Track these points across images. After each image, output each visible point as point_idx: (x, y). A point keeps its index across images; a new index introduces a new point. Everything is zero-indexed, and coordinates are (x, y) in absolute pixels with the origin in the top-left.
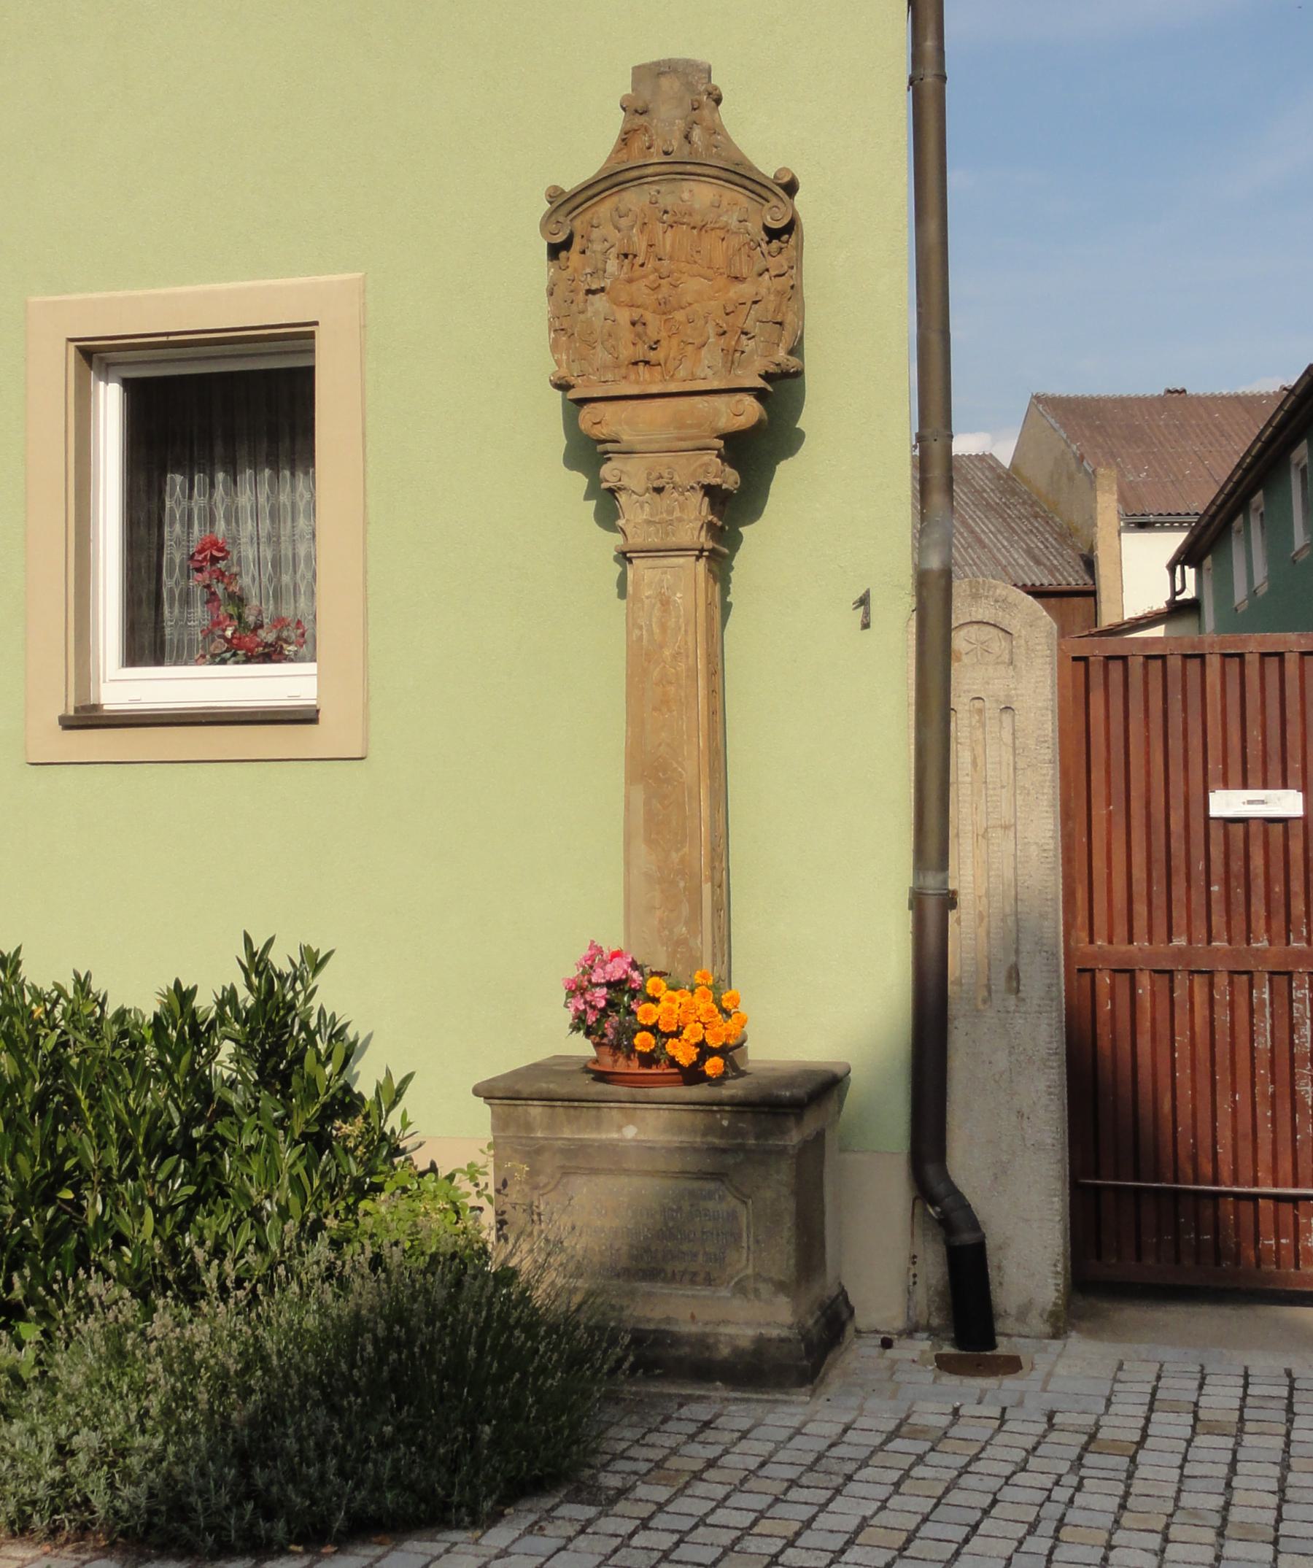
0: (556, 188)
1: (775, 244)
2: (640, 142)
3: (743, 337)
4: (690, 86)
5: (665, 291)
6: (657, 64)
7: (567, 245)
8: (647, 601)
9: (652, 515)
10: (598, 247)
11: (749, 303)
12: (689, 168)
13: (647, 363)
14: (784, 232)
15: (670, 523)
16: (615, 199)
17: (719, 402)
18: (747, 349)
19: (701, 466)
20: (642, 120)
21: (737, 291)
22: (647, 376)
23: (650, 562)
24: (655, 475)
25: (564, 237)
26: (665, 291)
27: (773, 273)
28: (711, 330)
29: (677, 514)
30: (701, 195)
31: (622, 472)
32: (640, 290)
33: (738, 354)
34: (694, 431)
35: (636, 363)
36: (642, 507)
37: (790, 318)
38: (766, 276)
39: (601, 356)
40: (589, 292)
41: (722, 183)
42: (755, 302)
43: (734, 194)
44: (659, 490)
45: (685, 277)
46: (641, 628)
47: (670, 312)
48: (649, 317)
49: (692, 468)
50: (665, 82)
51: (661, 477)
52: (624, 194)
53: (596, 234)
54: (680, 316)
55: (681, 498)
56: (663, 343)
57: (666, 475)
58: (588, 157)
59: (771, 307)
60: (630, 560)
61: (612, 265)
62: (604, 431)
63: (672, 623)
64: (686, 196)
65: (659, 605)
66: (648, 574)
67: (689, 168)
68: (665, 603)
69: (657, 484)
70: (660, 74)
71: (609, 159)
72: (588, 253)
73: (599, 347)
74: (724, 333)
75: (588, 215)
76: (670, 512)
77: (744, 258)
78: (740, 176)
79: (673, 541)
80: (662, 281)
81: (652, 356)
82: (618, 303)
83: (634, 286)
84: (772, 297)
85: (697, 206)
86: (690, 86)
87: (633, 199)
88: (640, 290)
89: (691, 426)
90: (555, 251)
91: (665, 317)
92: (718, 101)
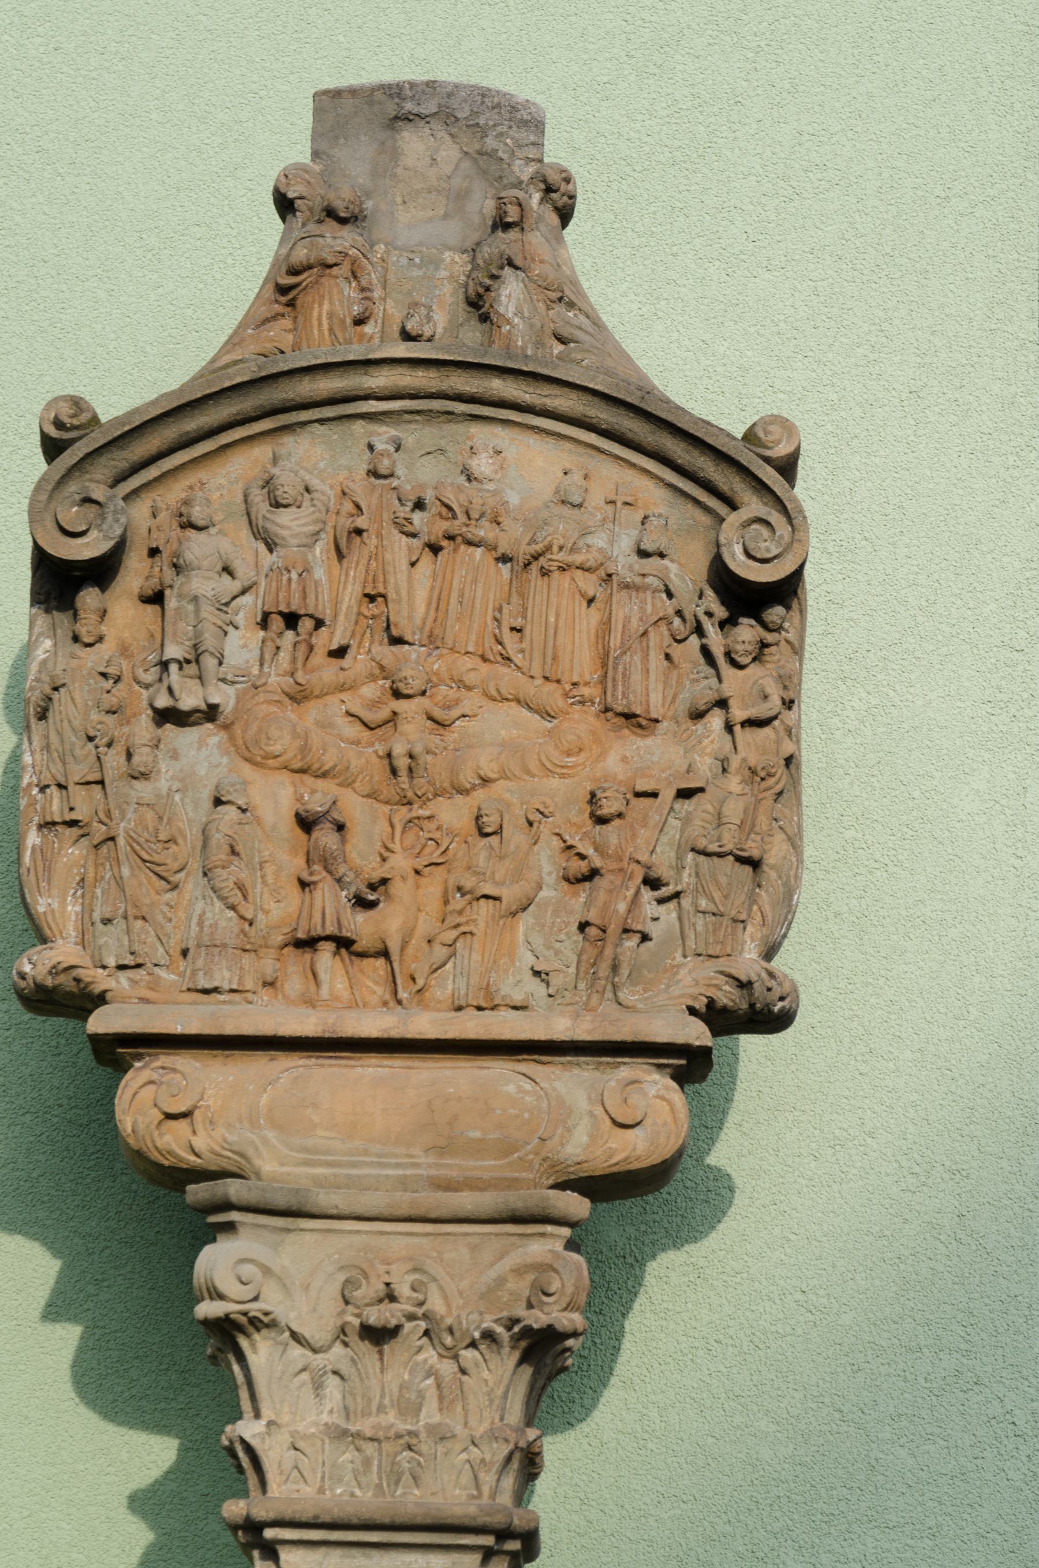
0: (77, 403)
1: (747, 632)
2: (332, 301)
3: (647, 894)
4: (486, 162)
5: (412, 733)
6: (394, 91)
7: (102, 571)
10: (206, 585)
11: (668, 794)
12: (499, 386)
13: (343, 943)
14: (757, 600)
16: (261, 452)
17: (571, 1083)
18: (655, 930)
19: (519, 1271)
20: (338, 240)
21: (625, 758)
22: (341, 986)
24: (364, 1292)
26: (412, 733)
27: (738, 713)
28: (547, 862)
29: (430, 1414)
30: (524, 469)
31: (266, 1271)
32: (330, 727)
34: (485, 1166)
35: (308, 944)
36: (318, 1387)
37: (775, 852)
38: (716, 720)
40: (169, 716)
42: (685, 794)
43: (630, 476)
44: (378, 1335)
45: (470, 702)
47: (423, 799)
48: (354, 807)
49: (493, 1273)
50: (413, 144)
52: (288, 440)
53: (198, 548)
54: (453, 814)
55: (448, 1368)
56: (399, 889)
57: (403, 1290)
58: (167, 323)
59: (734, 811)
61: (242, 646)
62: (200, 1142)
64: (482, 465)
67: (499, 386)
69: (375, 1316)
71: (234, 341)
72: (172, 602)
73: (193, 885)
74: (593, 874)
75: (173, 494)
76: (411, 1409)
77: (656, 661)
78: (642, 427)
79: (413, 1500)
80: (401, 705)
81: (360, 925)
83: (312, 711)
84: (734, 783)
85: (514, 499)
88: (330, 727)
89: (478, 1148)
90: (59, 583)
91: (403, 813)
92: (565, 215)
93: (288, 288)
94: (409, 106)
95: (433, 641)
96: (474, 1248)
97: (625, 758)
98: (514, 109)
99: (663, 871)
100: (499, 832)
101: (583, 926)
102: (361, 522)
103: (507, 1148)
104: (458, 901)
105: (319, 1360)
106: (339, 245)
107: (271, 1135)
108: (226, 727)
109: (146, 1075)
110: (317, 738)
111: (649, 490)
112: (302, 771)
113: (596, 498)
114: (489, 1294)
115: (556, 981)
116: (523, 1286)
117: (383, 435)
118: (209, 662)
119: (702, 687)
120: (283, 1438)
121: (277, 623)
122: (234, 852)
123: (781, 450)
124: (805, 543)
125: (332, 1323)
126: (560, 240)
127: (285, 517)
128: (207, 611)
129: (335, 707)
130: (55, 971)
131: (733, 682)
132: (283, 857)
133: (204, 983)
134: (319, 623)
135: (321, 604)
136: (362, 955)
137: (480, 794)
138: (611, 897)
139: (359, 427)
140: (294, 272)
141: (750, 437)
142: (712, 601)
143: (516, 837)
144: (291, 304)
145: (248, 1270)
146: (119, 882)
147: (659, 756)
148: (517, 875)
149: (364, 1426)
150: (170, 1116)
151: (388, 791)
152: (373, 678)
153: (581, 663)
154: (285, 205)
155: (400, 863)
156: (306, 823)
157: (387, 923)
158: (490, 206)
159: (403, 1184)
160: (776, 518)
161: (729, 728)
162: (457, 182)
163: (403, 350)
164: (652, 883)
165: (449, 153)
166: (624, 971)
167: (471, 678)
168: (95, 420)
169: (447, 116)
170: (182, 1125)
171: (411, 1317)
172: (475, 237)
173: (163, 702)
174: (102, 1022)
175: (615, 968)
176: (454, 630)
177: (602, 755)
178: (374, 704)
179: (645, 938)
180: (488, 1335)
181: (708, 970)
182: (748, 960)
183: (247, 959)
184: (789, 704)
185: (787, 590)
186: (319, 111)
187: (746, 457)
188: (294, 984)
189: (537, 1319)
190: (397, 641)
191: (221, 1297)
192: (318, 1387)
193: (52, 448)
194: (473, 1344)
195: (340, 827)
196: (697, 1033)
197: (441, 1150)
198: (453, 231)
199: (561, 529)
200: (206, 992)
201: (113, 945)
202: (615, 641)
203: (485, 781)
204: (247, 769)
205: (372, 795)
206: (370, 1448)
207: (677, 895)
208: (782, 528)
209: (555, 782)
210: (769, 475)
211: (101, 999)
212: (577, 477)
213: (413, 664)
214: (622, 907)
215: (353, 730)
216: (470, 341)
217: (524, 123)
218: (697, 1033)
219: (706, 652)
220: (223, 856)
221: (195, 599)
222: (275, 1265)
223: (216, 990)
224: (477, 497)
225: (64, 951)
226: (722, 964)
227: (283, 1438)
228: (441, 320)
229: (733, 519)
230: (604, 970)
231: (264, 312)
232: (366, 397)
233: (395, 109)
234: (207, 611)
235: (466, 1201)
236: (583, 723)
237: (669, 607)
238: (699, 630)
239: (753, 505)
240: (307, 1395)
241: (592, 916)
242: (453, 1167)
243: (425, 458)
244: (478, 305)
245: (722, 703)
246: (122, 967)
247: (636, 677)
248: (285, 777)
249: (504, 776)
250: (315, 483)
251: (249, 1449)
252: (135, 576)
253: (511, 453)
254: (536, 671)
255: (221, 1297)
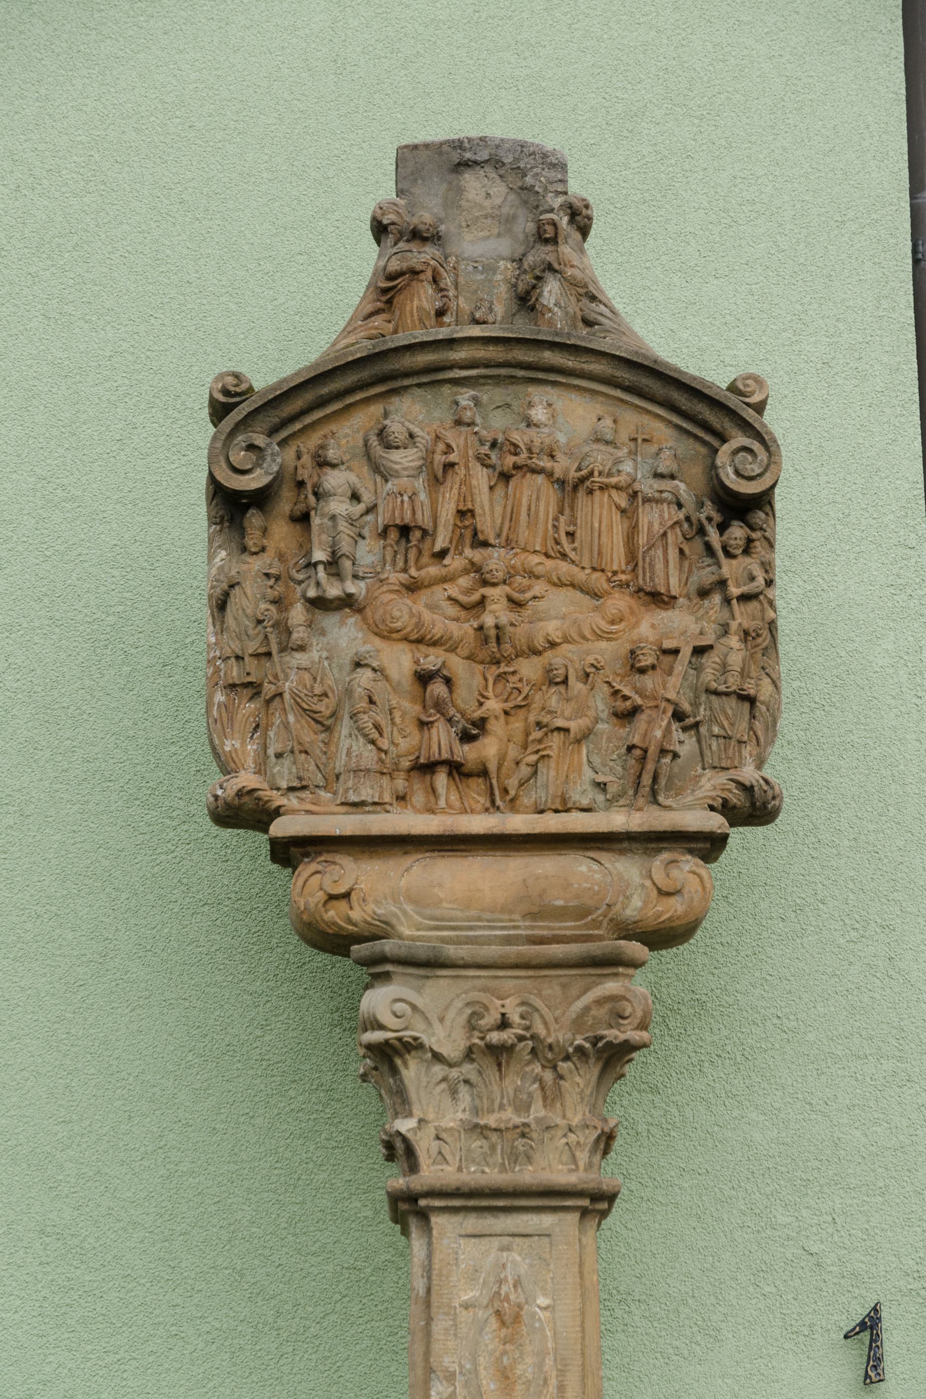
0: (237, 376)
1: (737, 532)
2: (423, 297)
3: (675, 726)
4: (528, 195)
5: (497, 613)
6: (458, 145)
7: (261, 499)
8: (464, 1316)
9: (476, 1111)
10: (339, 506)
11: (686, 652)
12: (549, 357)
14: (743, 509)
15: (524, 1132)
16: (376, 409)
18: (683, 750)
19: (599, 1002)
21: (651, 627)
22: (454, 797)
23: (472, 1223)
25: (266, 480)
26: (497, 613)
27: (734, 591)
28: (600, 703)
29: (538, 1111)
30: (567, 419)
31: (414, 1007)
33: (667, 760)
34: (567, 927)
36: (454, 1092)
37: (765, 691)
38: (717, 598)
39: (350, 746)
40: (319, 604)
41: (618, 393)
42: (700, 651)
43: (646, 420)
44: (499, 1054)
45: (539, 588)
46: (450, 1377)
47: (509, 661)
48: (458, 666)
49: (580, 1004)
50: (474, 185)
51: (504, 1024)
52: (395, 400)
53: (334, 480)
54: (529, 669)
55: (548, 1076)
56: (496, 727)
57: (515, 1018)
59: (736, 660)
60: (423, 1216)
61: (368, 553)
62: (356, 915)
63: (526, 1368)
64: (539, 414)
65: (494, 1323)
66: (470, 1250)
67: (549, 357)
68: (509, 1319)
69: (495, 1037)
70: (464, 165)
71: (348, 331)
72: (316, 521)
73: (345, 727)
75: (312, 441)
76: (523, 1107)
77: (673, 554)
79: (528, 1175)
80: (488, 591)
81: (468, 753)
82: (387, 634)
83: (424, 596)
84: (734, 641)
85: (562, 439)
86: (528, 195)
87: (412, 413)
89: (561, 913)
90: (232, 508)
91: (494, 671)
92: (584, 231)
93: (389, 291)
94: (468, 155)
95: (509, 544)
96: (564, 986)
97: (651, 627)
98: (545, 155)
99: (686, 707)
100: (565, 682)
101: (630, 748)
102: (453, 458)
103: (582, 912)
104: (537, 734)
105: (454, 1073)
106: (424, 257)
107: (409, 908)
108: (360, 611)
109: (314, 867)
110: (427, 616)
111: (660, 429)
112: (419, 641)
113: (624, 436)
114: (578, 1023)
115: (613, 789)
116: (601, 1013)
117: (465, 397)
118: (347, 564)
119: (705, 575)
120: (430, 1131)
121: (393, 535)
122: (371, 702)
123: (755, 399)
124: (778, 464)
125: (462, 1044)
126: (582, 251)
127: (396, 455)
128: (343, 526)
129: (439, 594)
130: (240, 793)
131: (729, 568)
132: (406, 704)
133: (353, 798)
134: (425, 532)
135: (424, 519)
136: (469, 775)
137: (549, 654)
138: (654, 728)
139: (446, 390)
140: (391, 277)
141: (733, 388)
142: (709, 509)
143: (576, 686)
144: (389, 302)
145: (400, 1007)
146: (286, 725)
147: (681, 624)
148: (580, 712)
149: (491, 1120)
150: (332, 897)
151: (483, 655)
152: (466, 572)
153: (617, 558)
154: (380, 230)
155: (493, 705)
156: (423, 678)
157: (489, 749)
158: (531, 227)
159: (508, 940)
160: (756, 446)
161: (727, 601)
162: (506, 210)
163: (476, 331)
164: (678, 716)
165: (499, 190)
166: (663, 781)
167: (539, 570)
168: (251, 389)
169: (495, 162)
170: (342, 905)
171: (521, 1038)
172: (521, 250)
173: (312, 593)
174: (281, 828)
175: (655, 779)
176: (523, 534)
177: (636, 625)
178: (468, 591)
179: (676, 755)
180: (580, 1050)
181: (722, 778)
182: (748, 773)
183: (385, 780)
184: (769, 583)
185: (763, 501)
186: (400, 162)
187: (733, 401)
188: (419, 798)
189: (615, 1035)
190: (485, 544)
191: (382, 1027)
192: (454, 1092)
193: (219, 411)
194: (567, 1058)
195: (448, 681)
196: (716, 822)
197: (533, 916)
198: (504, 246)
199: (600, 458)
200: (354, 805)
201: (284, 773)
202: (642, 539)
203: (553, 645)
204: (378, 642)
205: (470, 658)
206: (494, 1137)
207: (696, 725)
208: (762, 455)
209: (603, 644)
210: (749, 414)
211: (277, 812)
212: (608, 422)
213: (496, 560)
214: (658, 733)
215: (452, 611)
216: (522, 328)
217: (553, 166)
218: (716, 822)
219: (709, 548)
220: (364, 704)
221: (333, 518)
222: (419, 1002)
223: (363, 804)
224: (537, 437)
225: (247, 779)
226: (732, 774)
227: (430, 1131)
228: (499, 310)
229: (726, 449)
230: (647, 780)
231: (369, 308)
232: (451, 367)
233: (459, 159)
234: (343, 526)
235: (557, 950)
236: (619, 602)
237: (681, 515)
238: (702, 531)
239: (740, 440)
240: (447, 1101)
241: (636, 740)
242: (543, 928)
243: (494, 413)
244: (526, 301)
245: (722, 584)
246: (291, 789)
247: (659, 566)
248: (405, 646)
249: (567, 640)
250: (416, 430)
251: (405, 1140)
252: (285, 504)
253: (559, 405)
254: (586, 563)
255: (382, 1027)
